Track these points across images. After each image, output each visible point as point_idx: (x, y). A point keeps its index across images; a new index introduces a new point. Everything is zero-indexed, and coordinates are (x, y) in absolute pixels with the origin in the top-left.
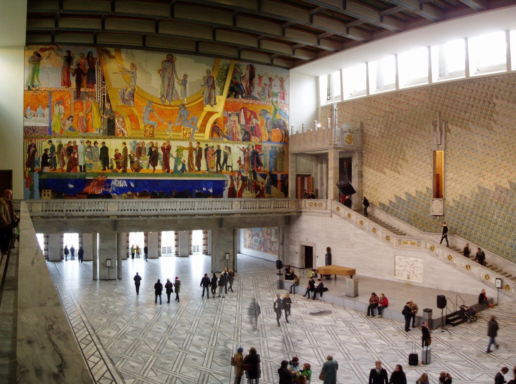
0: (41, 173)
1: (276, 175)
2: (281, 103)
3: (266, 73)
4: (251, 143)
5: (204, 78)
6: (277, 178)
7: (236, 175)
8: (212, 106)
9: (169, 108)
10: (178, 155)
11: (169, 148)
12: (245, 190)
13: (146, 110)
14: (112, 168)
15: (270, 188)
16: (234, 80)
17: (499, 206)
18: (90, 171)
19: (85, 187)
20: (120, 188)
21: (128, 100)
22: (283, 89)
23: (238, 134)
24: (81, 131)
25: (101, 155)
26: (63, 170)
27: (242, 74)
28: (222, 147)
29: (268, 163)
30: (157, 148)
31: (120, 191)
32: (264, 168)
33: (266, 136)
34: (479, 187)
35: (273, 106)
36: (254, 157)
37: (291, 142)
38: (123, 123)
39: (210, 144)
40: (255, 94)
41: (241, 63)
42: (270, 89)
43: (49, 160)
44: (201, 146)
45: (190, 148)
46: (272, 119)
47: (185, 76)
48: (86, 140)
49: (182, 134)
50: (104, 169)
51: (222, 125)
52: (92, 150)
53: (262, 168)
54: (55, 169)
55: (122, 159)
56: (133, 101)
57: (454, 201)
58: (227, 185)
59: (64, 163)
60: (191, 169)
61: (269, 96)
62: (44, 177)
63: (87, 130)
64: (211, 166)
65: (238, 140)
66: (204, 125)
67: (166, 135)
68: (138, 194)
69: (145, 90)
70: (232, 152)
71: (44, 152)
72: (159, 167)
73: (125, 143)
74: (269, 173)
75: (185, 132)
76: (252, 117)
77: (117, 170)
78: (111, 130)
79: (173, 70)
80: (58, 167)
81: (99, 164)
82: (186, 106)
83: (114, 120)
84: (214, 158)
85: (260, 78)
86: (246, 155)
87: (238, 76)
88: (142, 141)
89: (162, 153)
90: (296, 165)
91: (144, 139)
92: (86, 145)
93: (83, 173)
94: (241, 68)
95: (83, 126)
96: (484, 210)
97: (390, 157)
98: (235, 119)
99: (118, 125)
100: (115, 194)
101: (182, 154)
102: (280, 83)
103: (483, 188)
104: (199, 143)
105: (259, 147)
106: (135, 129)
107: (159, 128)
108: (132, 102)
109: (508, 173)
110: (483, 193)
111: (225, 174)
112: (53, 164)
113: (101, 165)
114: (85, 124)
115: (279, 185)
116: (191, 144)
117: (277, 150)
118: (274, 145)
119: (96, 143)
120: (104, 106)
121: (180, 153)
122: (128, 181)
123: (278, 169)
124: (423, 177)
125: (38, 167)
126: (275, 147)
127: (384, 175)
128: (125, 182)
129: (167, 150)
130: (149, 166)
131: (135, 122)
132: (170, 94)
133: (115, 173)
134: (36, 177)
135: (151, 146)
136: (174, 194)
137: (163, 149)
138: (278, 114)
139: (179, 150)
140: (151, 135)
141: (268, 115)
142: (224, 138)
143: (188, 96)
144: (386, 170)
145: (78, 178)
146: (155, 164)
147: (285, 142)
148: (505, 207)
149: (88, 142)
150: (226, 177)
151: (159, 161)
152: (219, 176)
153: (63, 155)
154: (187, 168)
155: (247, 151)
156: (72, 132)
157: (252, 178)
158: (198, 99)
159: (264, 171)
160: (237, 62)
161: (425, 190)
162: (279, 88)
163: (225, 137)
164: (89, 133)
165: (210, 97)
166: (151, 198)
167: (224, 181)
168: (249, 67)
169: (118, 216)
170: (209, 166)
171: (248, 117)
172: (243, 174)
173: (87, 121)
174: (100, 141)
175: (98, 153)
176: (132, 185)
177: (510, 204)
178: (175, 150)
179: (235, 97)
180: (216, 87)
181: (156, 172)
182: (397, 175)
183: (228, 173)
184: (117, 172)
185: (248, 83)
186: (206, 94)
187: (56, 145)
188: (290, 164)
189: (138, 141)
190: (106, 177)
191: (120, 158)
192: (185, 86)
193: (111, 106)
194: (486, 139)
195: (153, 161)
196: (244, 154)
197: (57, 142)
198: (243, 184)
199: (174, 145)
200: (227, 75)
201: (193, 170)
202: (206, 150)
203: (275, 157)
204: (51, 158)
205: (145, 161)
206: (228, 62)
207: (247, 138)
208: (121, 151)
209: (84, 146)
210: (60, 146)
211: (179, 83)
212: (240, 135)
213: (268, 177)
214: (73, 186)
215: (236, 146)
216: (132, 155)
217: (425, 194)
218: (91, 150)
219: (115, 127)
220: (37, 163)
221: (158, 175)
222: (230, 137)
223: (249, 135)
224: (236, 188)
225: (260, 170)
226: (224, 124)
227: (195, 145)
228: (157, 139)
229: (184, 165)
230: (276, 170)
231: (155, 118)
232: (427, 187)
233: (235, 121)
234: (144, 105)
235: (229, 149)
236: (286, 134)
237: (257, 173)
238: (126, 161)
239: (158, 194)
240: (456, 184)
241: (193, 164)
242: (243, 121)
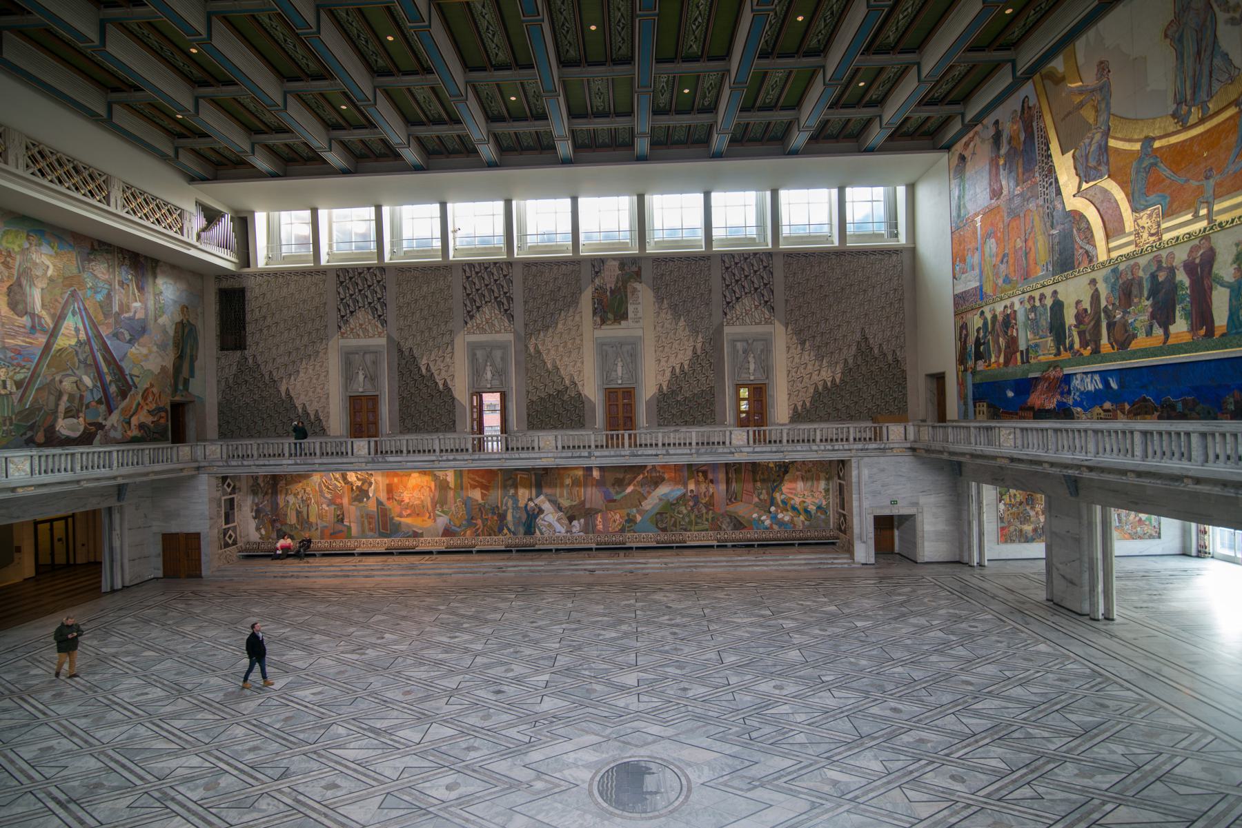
0: (974, 373)
11: (1210, 257)
13: (1137, 172)
14: (1071, 347)
20: (1089, 392)
21: (1095, 168)
26: (999, 365)
30: (1172, 271)
31: (1092, 400)
48: (1027, 296)
50: (1058, 353)
62: (978, 379)
63: (1026, 277)
67: (1196, 218)
68: (1127, 407)
72: (1180, 326)
73: (1093, 282)
81: (1050, 341)
88: (1132, 262)
89: (1187, 282)
93: (1026, 366)
100: (1079, 409)
108: (1103, 168)
119: (1042, 297)
122: (1104, 375)
125: (970, 363)
128: (1097, 377)
130: (1151, 327)
132: (1205, 81)
133: (1078, 359)
135: (1154, 268)
136: (1232, 407)
137: (1189, 267)
140: (1152, 239)
151: (1178, 307)
153: (998, 336)
156: (1007, 287)
166: (1160, 418)
169: (1012, 460)
176: (1114, 385)
178: (1230, 259)
181: (1171, 341)
187: (989, 316)
191: (1086, 320)
195: (1163, 315)
205: (1140, 314)
208: (1086, 305)
210: (994, 317)
231: (1163, 180)
239: (1180, 407)
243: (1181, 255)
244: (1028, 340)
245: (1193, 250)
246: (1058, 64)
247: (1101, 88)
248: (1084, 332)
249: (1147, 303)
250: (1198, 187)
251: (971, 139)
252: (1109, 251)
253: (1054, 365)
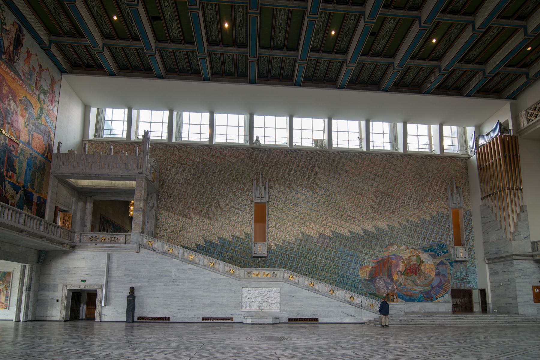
17: (322, 249)
29: (24, 172)
32: (18, 177)
34: (303, 235)
57: (276, 245)
96: (308, 252)
97: (199, 204)
103: (307, 235)
109: (330, 225)
110: (307, 239)
117: (37, 161)
124: (241, 224)
127: (189, 220)
144: (192, 215)
147: (47, 157)
148: (328, 250)
159: (17, 182)
161: (244, 235)
177: (333, 248)
182: (207, 221)
194: (310, 198)
203: (33, 170)
217: (243, 239)
232: (245, 233)
240: (279, 231)
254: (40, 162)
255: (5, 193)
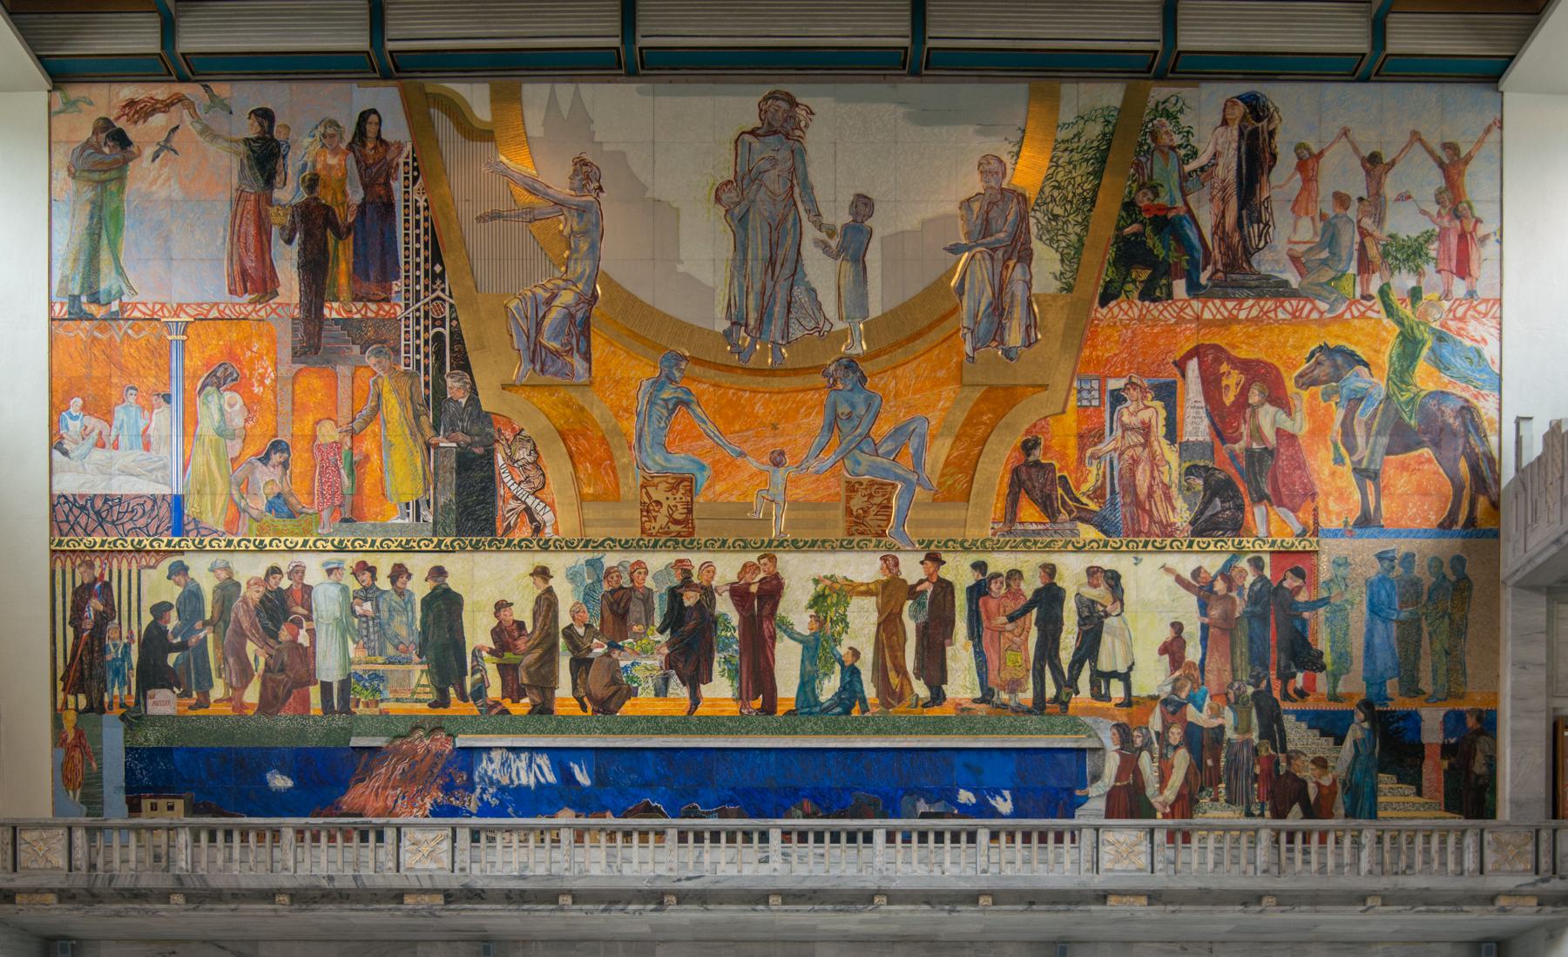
0: (134, 719)
1: (1413, 718)
2: (1446, 295)
3: (1345, 132)
4: (1247, 543)
5: (967, 203)
6: (1418, 731)
7: (1155, 723)
8: (1006, 352)
9: (776, 383)
10: (819, 621)
11: (773, 590)
12: (1205, 801)
13: (651, 403)
14: (479, 692)
15: (1374, 793)
16: (1143, 200)
18: (374, 711)
19: (345, 788)
20: (522, 790)
21: (556, 354)
22: (1456, 214)
23: (1168, 498)
24: (325, 514)
25: (424, 632)
27: (1194, 154)
28: (1072, 570)
30: (708, 592)
32: (1335, 678)
33: (1342, 496)
35: (1386, 321)
36: (1263, 619)
37: (1510, 522)
38: (533, 473)
39: (999, 563)
40: (1272, 262)
41: (1187, 92)
42: (1367, 223)
43: (172, 659)
44: (945, 573)
45: (885, 585)
46: (1388, 397)
47: (863, 205)
48: (350, 560)
49: (840, 512)
50: (443, 701)
51: (1073, 453)
52: (383, 607)
53: (1321, 677)
54: (204, 702)
55: (528, 651)
56: (587, 357)
58: (1097, 777)
59: (245, 673)
60: (890, 695)
61: (1365, 266)
62: (151, 737)
63: (352, 516)
64: (1006, 675)
65: (1167, 530)
66: (965, 465)
69: (645, 296)
70: (1130, 596)
71: (147, 618)
72: (720, 690)
73: (542, 573)
74: (1367, 705)
75: (857, 503)
76: (1254, 397)
77: (507, 703)
78: (472, 510)
79: (797, 174)
80: (218, 691)
81: (418, 675)
82: (866, 367)
83: (489, 456)
84: (1025, 630)
85: (1307, 163)
86: (1215, 612)
87: (1165, 172)
88: (633, 558)
89: (735, 619)
90: (1550, 656)
91: (639, 548)
92: (354, 585)
93: (339, 721)
94: (1184, 120)
95: (336, 490)
98: (1145, 415)
99: (508, 481)
101: (843, 620)
102: (1437, 179)
104: (934, 559)
105: (1296, 562)
106: (596, 498)
107: (719, 487)
108: (579, 364)
111: (1089, 720)
112: (194, 679)
113: (424, 681)
114: (346, 481)
115: (1433, 771)
116: (891, 564)
117: (1420, 570)
118: (1401, 546)
120: (439, 391)
121: (831, 614)
123: (1426, 684)
125: (119, 693)
126: (1408, 558)
128: (543, 761)
129: (760, 600)
130: (666, 680)
131: (597, 464)
133: (496, 717)
134: (113, 739)
135: (676, 581)
137: (739, 594)
138: (1422, 367)
139: (830, 597)
140: (674, 528)
141: (1358, 379)
142: (1081, 527)
143: (875, 310)
145: (313, 742)
146: (696, 677)
147: (1471, 521)
149: (363, 567)
150: (1091, 733)
151: (718, 657)
152: (1050, 731)
153: (241, 635)
154: (870, 691)
155: (1220, 586)
156: (279, 523)
157: (1255, 736)
158: (931, 327)
159: (1334, 698)
160: (1159, 92)
162: (1434, 209)
163: (1085, 517)
164: (367, 525)
165: (999, 310)
167: (1081, 752)
168: (1240, 110)
170: (994, 679)
171: (1229, 399)
172: (1191, 713)
173: (355, 468)
174: (419, 565)
175: (410, 625)
176: (583, 778)
178: (806, 599)
179: (1147, 294)
180: (1036, 245)
181: (702, 710)
183: (1104, 714)
184: (506, 712)
185: (1233, 204)
186: (979, 298)
188: (1508, 650)
189: (611, 560)
190: (452, 736)
191: (522, 644)
192: (859, 261)
193: (474, 390)
196: (1204, 608)
197: (212, 570)
198: (1197, 764)
199: (801, 574)
200: (1098, 174)
201: (900, 698)
202: (977, 592)
203: (1404, 615)
204: (183, 647)
205: (645, 656)
206: (1111, 94)
207: (1219, 513)
208: (523, 611)
209: (345, 589)
210: (228, 590)
211: (826, 247)
212: (1180, 503)
213: (1358, 730)
214: (290, 783)
215: (1151, 562)
216: (581, 631)
218: (377, 609)
219: (494, 493)
220: (117, 672)
221: (713, 725)
222: (1121, 515)
223: (1236, 495)
224: (1151, 790)
225: (1302, 694)
226: (1082, 449)
227: (912, 569)
228: (706, 547)
229: (851, 674)
230: (1411, 687)
231: (699, 437)
233: (1146, 429)
234: (640, 372)
235: (1114, 580)
236: (1483, 475)
237: (1285, 705)
238: (550, 656)
241: (901, 670)
242: (1196, 426)
243: (727, 568)
244: (347, 661)
245: (746, 567)
246: (476, 97)
247: (582, 211)
248: (515, 667)
249: (658, 637)
250: (761, 472)
251: (166, 106)
252: (583, 524)
253: (436, 728)
254: (1436, 563)
255: (1289, 759)
